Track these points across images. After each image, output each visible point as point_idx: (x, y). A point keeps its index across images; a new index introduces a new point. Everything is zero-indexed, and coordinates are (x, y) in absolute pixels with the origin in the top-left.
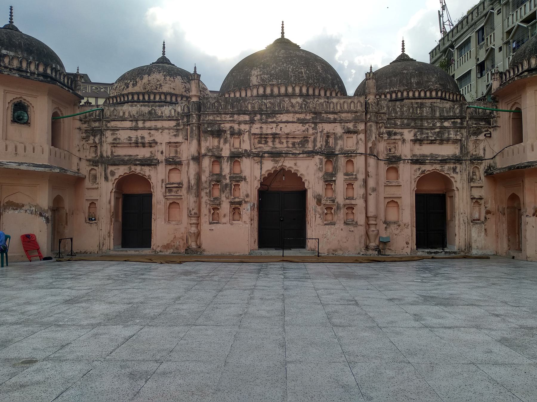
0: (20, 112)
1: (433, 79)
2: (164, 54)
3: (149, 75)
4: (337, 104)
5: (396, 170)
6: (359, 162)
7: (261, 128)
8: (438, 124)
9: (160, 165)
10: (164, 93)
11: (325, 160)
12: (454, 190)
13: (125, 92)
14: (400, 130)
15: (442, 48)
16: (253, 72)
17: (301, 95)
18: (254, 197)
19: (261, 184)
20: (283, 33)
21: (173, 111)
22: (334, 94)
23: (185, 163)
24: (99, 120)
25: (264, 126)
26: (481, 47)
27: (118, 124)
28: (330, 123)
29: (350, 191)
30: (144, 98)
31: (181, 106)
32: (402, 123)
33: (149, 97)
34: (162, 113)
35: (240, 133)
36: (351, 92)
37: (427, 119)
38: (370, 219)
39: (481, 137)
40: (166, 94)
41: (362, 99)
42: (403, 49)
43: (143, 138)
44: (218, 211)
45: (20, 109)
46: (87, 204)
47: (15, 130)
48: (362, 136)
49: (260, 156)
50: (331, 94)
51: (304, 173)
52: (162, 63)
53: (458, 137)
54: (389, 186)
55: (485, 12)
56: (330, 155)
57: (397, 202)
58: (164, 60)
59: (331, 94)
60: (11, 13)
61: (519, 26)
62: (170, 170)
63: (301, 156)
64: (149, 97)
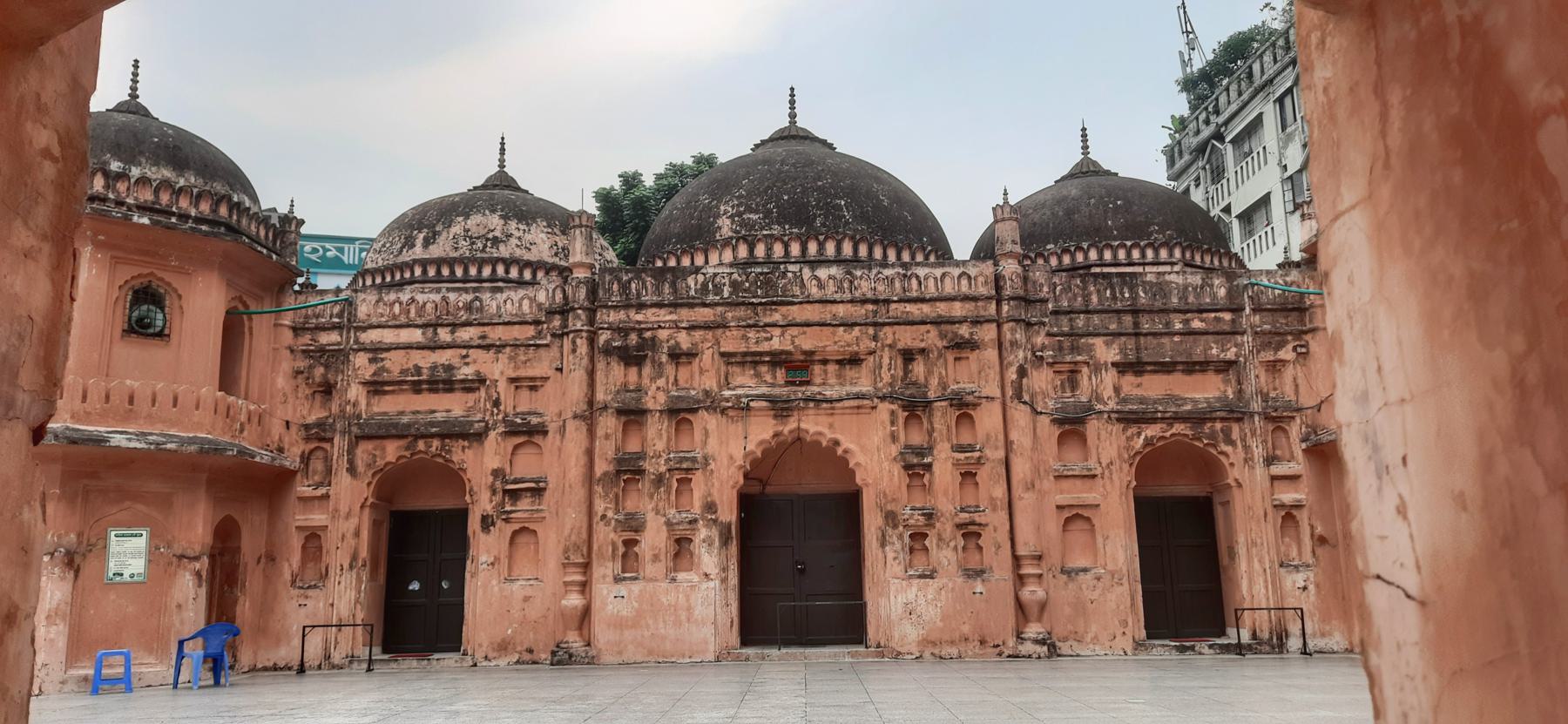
0: (145, 307)
2: (502, 166)
3: (467, 217)
4: (926, 278)
5: (1083, 439)
6: (988, 419)
8: (1178, 326)
9: (492, 434)
10: (503, 260)
11: (902, 415)
12: (1229, 486)
13: (407, 256)
15: (1195, 141)
17: (838, 261)
18: (729, 513)
19: (746, 476)
20: (793, 116)
21: (526, 303)
22: (920, 258)
23: (552, 427)
25: (752, 334)
27: (388, 336)
29: (970, 489)
30: (453, 272)
33: (466, 270)
34: (499, 307)
35: (691, 355)
36: (962, 247)
38: (1024, 562)
39: (1287, 354)
40: (508, 263)
41: (988, 268)
42: (1085, 147)
44: (636, 549)
45: (145, 302)
46: (296, 542)
47: (134, 353)
48: (991, 354)
49: (742, 409)
50: (913, 258)
51: (852, 446)
53: (1230, 354)
54: (1067, 477)
56: (915, 407)
57: (1088, 519)
58: (502, 182)
59: (913, 258)
60: (135, 75)
62: (516, 447)
63: (847, 403)
64: (466, 270)
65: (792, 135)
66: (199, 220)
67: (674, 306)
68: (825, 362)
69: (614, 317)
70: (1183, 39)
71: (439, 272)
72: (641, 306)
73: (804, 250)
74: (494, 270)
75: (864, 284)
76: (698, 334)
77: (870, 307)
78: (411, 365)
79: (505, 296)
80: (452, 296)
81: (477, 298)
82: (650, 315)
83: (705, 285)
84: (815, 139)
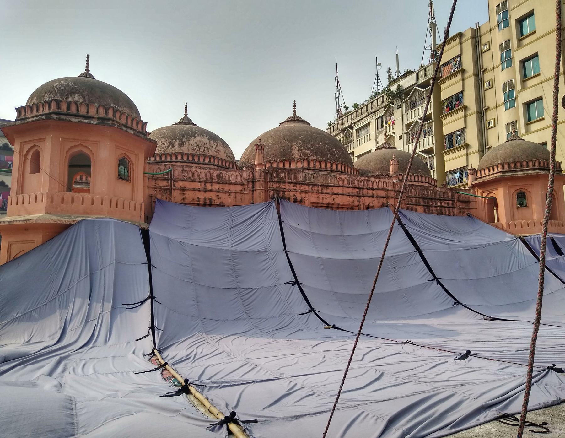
1: (421, 168)
2: (186, 114)
3: (195, 137)
7: (318, 197)
8: (439, 204)
13: (170, 151)
14: (415, 207)
15: (341, 127)
16: (294, 147)
20: (295, 111)
21: (239, 176)
24: (167, 180)
25: (321, 196)
26: (380, 132)
27: (187, 185)
28: (370, 197)
30: (193, 159)
31: (247, 173)
32: (416, 201)
33: (199, 159)
34: (229, 177)
37: (432, 199)
43: (210, 200)
52: (184, 123)
55: (385, 104)
58: (186, 121)
61: (417, 121)
64: (199, 159)
65: (295, 119)
66: (139, 132)
67: (295, 184)
68: (343, 208)
69: (275, 186)
70: (335, 90)
71: (188, 159)
72: (284, 182)
73: (326, 166)
74: (210, 160)
75: (356, 182)
76: (303, 195)
77: (357, 190)
78: (196, 197)
79: (231, 173)
80: (212, 171)
81: (221, 173)
82: (287, 186)
83: (305, 177)
84: (305, 121)
